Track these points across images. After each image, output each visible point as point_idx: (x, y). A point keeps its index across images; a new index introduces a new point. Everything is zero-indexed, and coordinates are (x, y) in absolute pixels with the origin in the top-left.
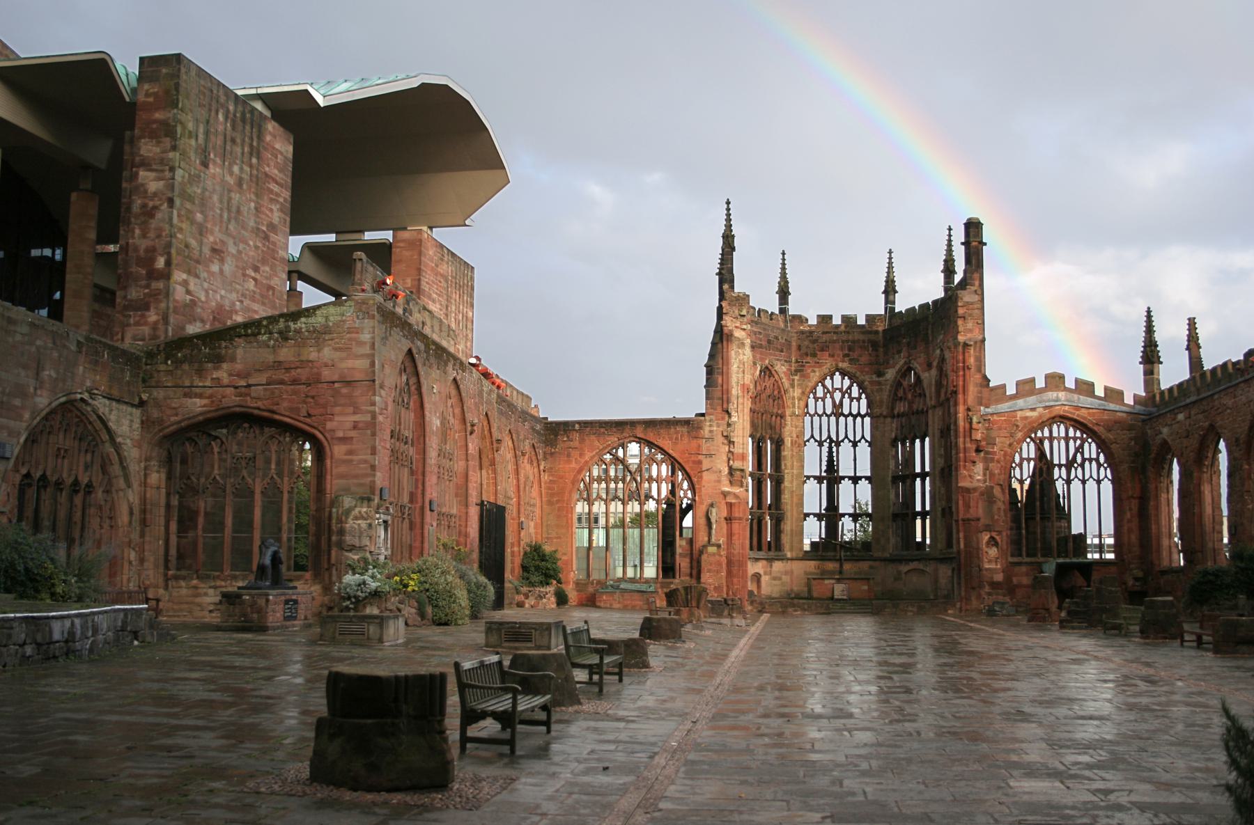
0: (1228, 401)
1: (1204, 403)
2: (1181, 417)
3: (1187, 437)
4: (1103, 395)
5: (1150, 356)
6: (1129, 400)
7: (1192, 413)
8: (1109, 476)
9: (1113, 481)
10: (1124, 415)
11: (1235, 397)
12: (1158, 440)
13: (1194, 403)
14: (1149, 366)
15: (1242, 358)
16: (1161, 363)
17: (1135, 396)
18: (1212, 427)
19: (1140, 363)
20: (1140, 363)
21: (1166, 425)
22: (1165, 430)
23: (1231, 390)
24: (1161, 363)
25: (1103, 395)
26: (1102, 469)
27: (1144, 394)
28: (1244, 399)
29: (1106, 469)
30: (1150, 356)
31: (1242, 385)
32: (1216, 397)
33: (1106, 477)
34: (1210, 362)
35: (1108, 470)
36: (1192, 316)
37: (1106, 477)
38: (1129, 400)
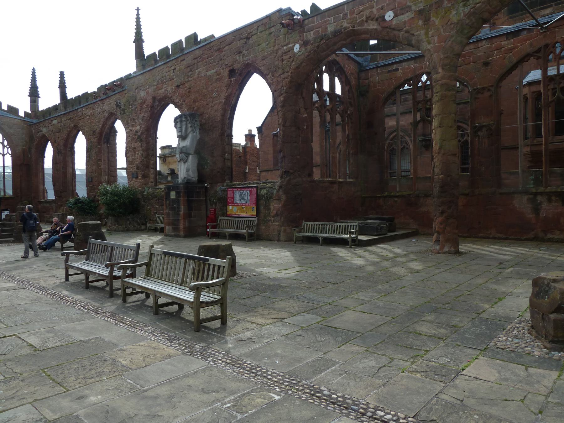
0: (88, 112)
1: (71, 114)
2: (55, 122)
3: (60, 132)
4: (6, 109)
5: (34, 94)
6: (22, 114)
7: (63, 120)
8: (10, 152)
9: (12, 155)
10: (19, 121)
11: (93, 109)
12: (40, 134)
13: (64, 114)
14: (33, 98)
15: (96, 90)
16: (40, 97)
17: (26, 113)
18: (76, 126)
19: (28, 96)
20: (28, 96)
21: (45, 127)
22: (44, 130)
23: (91, 106)
24: (40, 97)
25: (6, 109)
26: (6, 149)
27: (30, 112)
28: (99, 110)
29: (8, 148)
30: (34, 94)
31: (99, 102)
32: (79, 110)
33: (8, 153)
34: (71, 94)
35: (9, 149)
36: (62, 71)
37: (8, 153)
38: (22, 114)
